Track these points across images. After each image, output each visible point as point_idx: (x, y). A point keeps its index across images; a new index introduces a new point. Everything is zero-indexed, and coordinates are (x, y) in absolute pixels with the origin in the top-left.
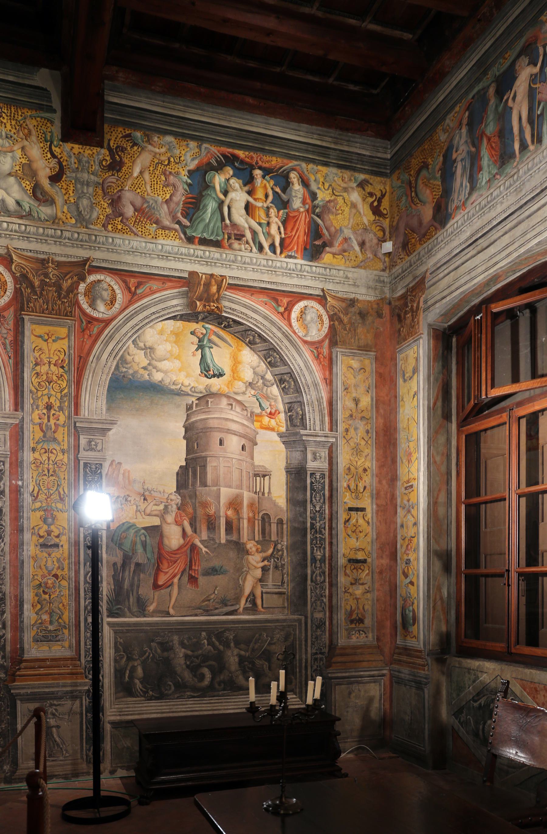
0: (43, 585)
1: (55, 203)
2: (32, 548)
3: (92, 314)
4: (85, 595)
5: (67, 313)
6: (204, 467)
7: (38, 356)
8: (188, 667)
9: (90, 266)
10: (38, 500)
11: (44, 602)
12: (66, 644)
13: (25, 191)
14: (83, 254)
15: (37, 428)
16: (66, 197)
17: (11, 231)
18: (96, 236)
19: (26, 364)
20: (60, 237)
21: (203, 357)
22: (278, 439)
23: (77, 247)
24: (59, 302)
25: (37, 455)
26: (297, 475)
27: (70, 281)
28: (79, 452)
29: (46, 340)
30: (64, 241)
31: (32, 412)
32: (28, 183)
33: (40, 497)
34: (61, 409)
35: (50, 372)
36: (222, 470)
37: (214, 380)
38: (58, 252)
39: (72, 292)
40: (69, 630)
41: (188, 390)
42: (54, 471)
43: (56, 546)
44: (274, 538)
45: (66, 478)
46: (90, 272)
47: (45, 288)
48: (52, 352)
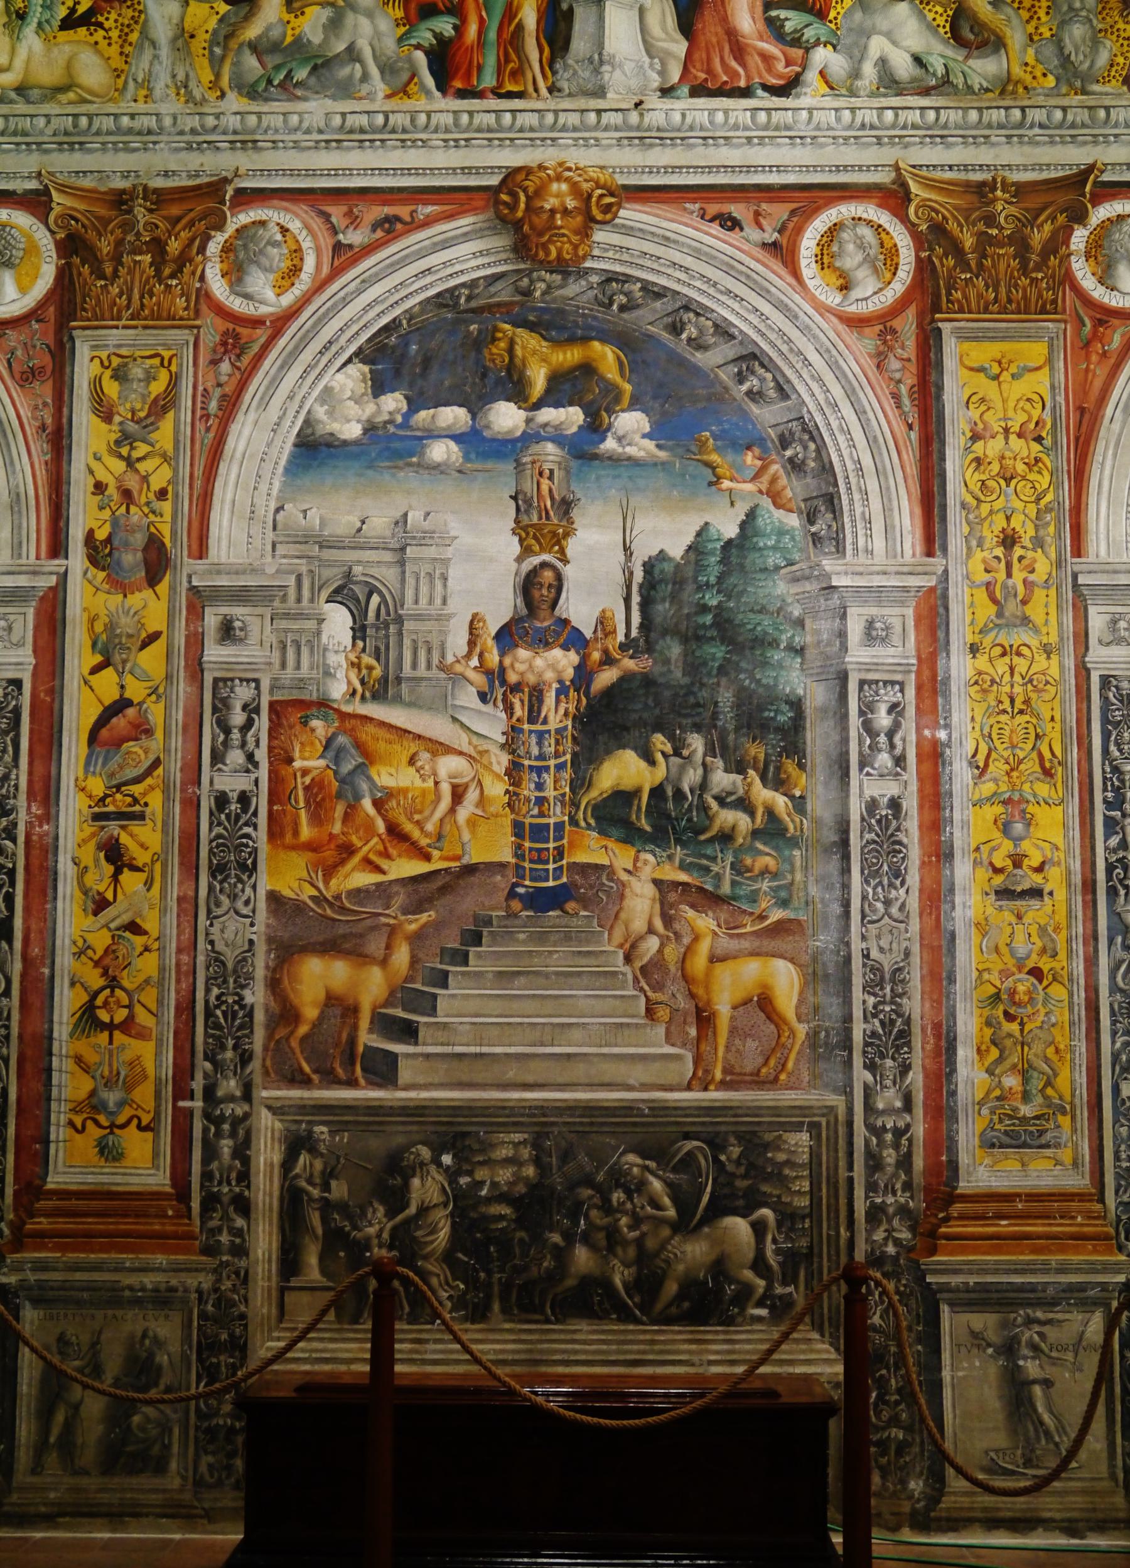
0: (1004, 997)
1: (1005, 46)
2: (975, 899)
3: (1106, 300)
4: (1114, 1023)
5: (1044, 305)
7: (976, 417)
9: (1095, 183)
10: (987, 777)
11: (1008, 1043)
12: (1066, 1155)
13: (933, 29)
14: (1078, 156)
15: (982, 595)
16: (1030, 29)
17: (904, 127)
18: (1107, 109)
19: (949, 439)
20: (1021, 125)
23: (1063, 143)
24: (1024, 281)
25: (982, 662)
27: (1048, 227)
28: (1087, 649)
29: (997, 377)
30: (1031, 133)
31: (969, 556)
32: (940, 10)
33: (991, 768)
34: (1038, 543)
35: (1008, 454)
38: (1017, 160)
39: (1055, 252)
40: (1073, 1118)
42: (1027, 702)
43: (1036, 893)
45: (1057, 718)
46: (1097, 199)
47: (990, 250)
48: (1011, 404)
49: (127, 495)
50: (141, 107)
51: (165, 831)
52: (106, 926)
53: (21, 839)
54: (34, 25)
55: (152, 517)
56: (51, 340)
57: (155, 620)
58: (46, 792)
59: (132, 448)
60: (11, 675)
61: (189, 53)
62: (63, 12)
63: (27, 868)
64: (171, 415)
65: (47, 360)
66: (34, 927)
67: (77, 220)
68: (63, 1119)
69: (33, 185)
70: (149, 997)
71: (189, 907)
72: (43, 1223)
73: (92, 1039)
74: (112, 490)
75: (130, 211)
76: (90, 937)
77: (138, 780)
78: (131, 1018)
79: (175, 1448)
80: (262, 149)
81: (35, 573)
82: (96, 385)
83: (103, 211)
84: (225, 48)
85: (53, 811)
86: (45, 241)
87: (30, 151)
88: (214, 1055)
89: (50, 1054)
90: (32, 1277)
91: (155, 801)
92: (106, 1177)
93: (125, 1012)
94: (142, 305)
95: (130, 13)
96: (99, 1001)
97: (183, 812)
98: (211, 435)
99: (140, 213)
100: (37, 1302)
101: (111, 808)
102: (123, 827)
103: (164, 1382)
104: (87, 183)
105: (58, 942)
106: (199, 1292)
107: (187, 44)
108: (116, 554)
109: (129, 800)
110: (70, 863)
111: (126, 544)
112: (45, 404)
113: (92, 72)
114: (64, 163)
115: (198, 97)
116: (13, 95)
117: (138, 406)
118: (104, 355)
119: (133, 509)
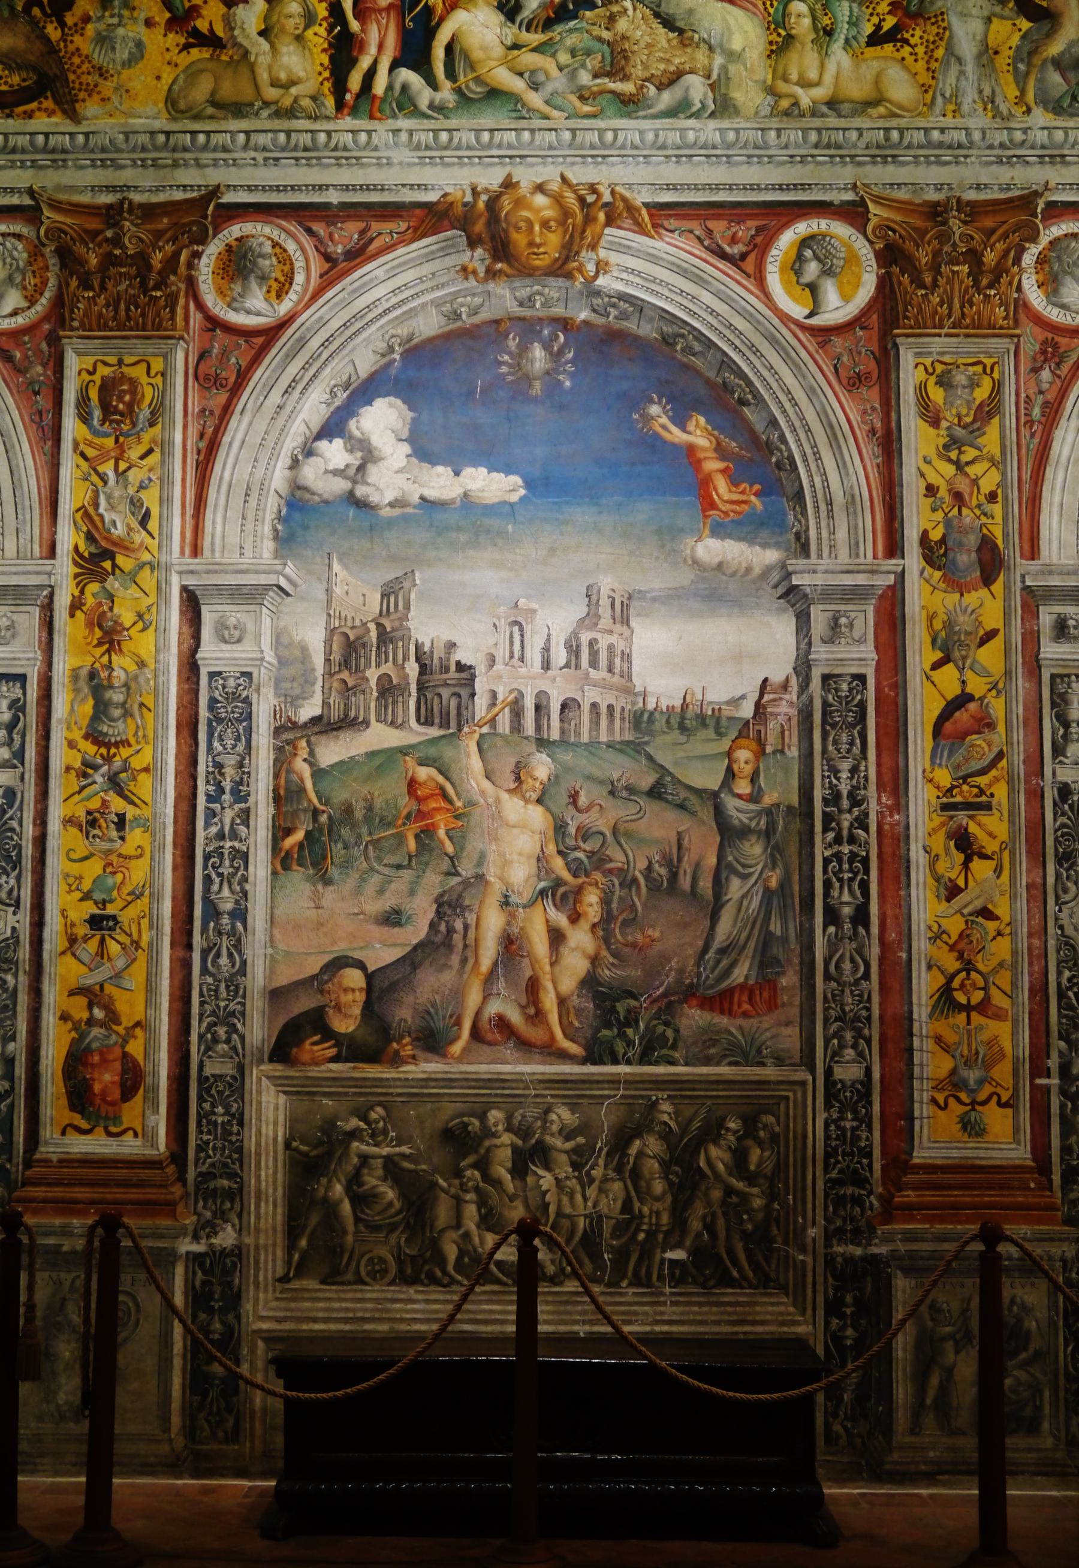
49: (958, 497)
50: (949, 121)
51: (1011, 822)
52: (960, 912)
53: (873, 828)
54: (842, 41)
55: (984, 519)
56: (875, 348)
57: (992, 618)
58: (895, 784)
59: (961, 452)
60: (854, 670)
61: (994, 69)
62: (869, 29)
63: (880, 856)
64: (996, 421)
65: (873, 366)
66: (889, 912)
67: (894, 231)
68: (926, 1096)
69: (849, 196)
70: (1004, 980)
71: (1038, 893)
72: (910, 1196)
73: (951, 1020)
74: (943, 493)
75: (945, 223)
76: (944, 922)
77: (983, 772)
78: (986, 1000)
79: (1047, 1410)
80: (1069, 164)
81: (872, 572)
82: (922, 390)
83: (918, 222)
84: (1029, 64)
85: (903, 802)
86: (864, 250)
87: (845, 164)
88: (1068, 1035)
89: (911, 1035)
90: (902, 1247)
91: (1001, 792)
92: (970, 1151)
93: (982, 993)
94: (963, 313)
95: (934, 29)
96: (956, 984)
97: (1028, 802)
98: (1036, 440)
99: (955, 224)
100: (907, 1271)
101: (959, 799)
102: (971, 817)
103: (1033, 1347)
104: (902, 195)
105: (914, 928)
106: (1063, 1260)
107: (992, 60)
108: (951, 555)
109: (975, 790)
110: (921, 852)
111: (961, 545)
112: (873, 409)
113: (901, 88)
114: (878, 175)
115: (1005, 112)
116: (824, 109)
117: (964, 412)
118: (928, 362)
119: (965, 511)
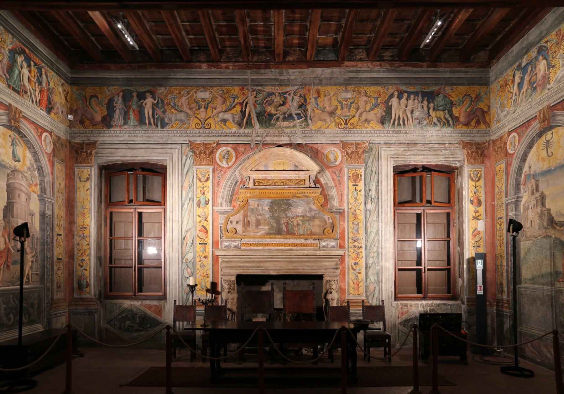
6: (13, 207)
8: (5, 314)
21: (13, 149)
22: (37, 197)
26: (43, 215)
36: (19, 210)
37: (17, 162)
41: (8, 165)
44: (36, 247)
